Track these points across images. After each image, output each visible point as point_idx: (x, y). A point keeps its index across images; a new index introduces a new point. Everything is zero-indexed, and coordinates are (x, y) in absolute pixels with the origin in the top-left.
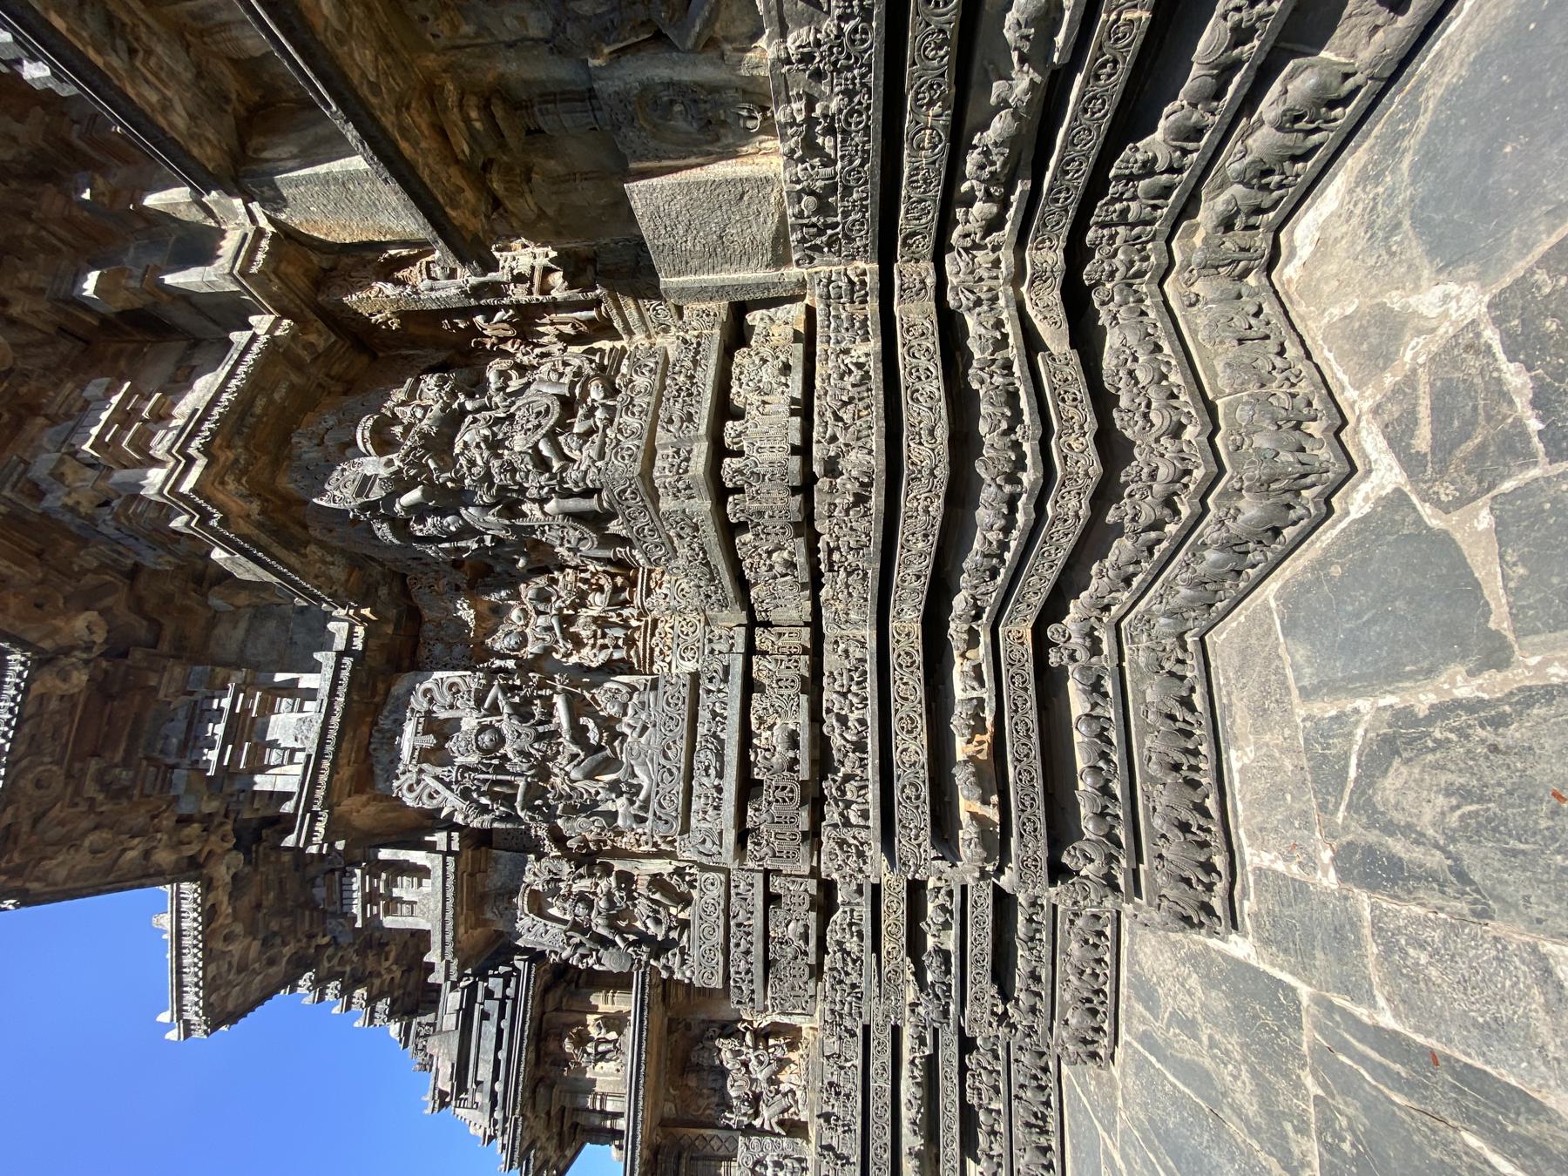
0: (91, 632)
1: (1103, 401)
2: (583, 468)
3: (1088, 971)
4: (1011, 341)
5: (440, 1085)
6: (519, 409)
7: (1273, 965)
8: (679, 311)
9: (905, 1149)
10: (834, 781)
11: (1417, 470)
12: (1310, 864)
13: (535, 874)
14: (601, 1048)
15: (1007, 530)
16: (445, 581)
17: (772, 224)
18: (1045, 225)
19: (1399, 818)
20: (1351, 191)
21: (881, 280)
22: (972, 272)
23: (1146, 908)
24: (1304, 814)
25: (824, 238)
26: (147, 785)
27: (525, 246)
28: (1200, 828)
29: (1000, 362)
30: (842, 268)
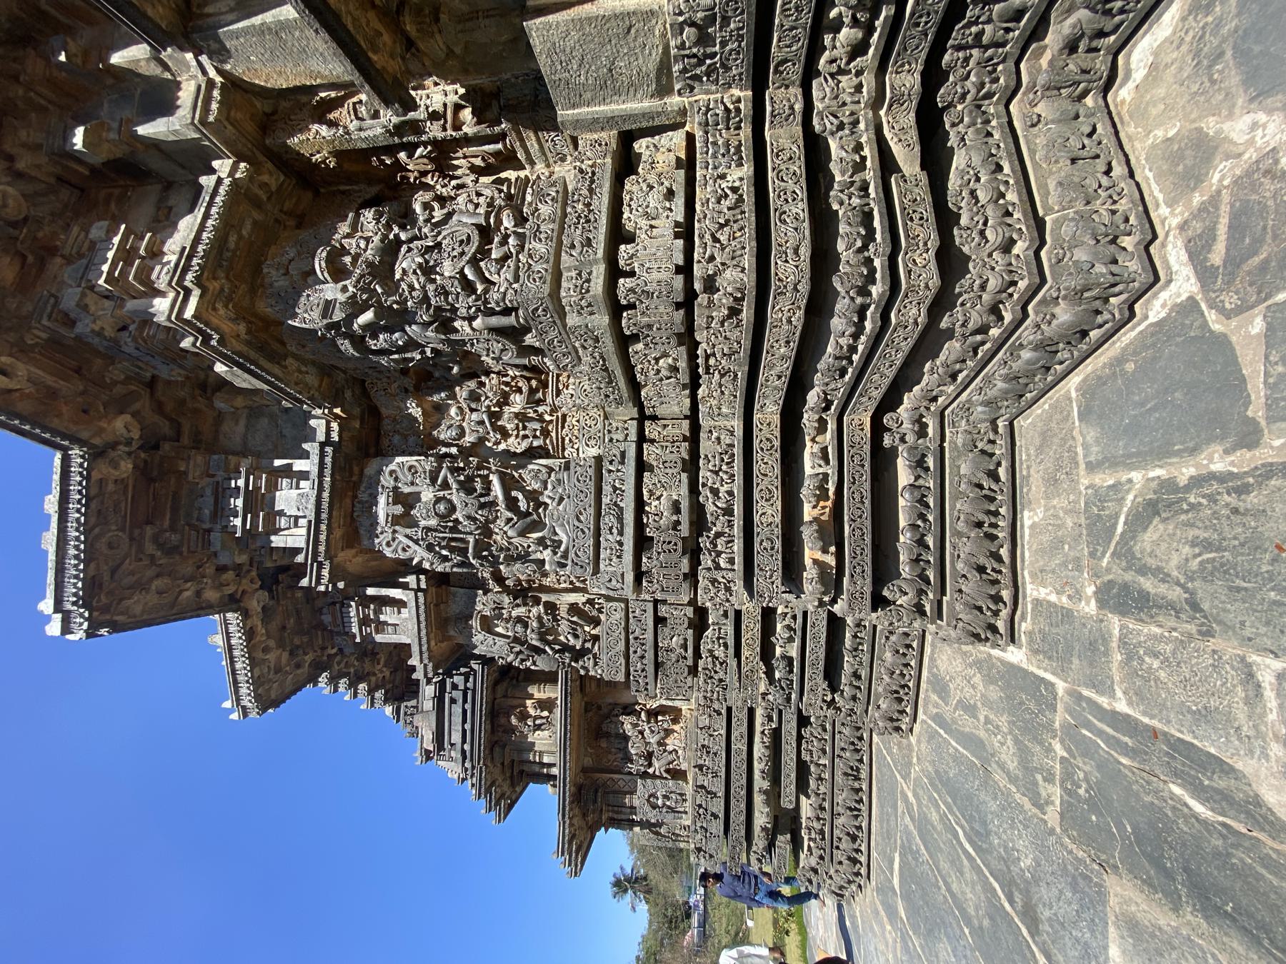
0: (129, 431)
2: (502, 290)
3: (898, 672)
4: (869, 163)
5: (425, 745)
6: (444, 238)
7: (1039, 667)
8: (575, 141)
9: (756, 789)
10: (708, 537)
11: (1209, 281)
12: (1077, 596)
13: (483, 604)
14: (538, 722)
15: (855, 336)
16: (396, 385)
17: (656, 55)
18: (905, 49)
19: (1152, 562)
21: (754, 107)
22: (836, 97)
23: (946, 627)
24: (1077, 560)
25: (704, 68)
26: (192, 544)
27: (436, 84)
28: (993, 570)
29: (857, 185)
30: (719, 95)
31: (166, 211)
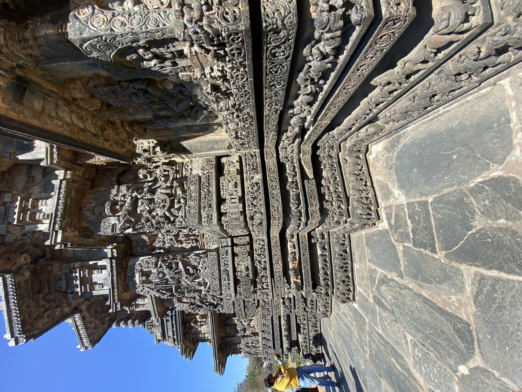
1: (321, 197)
5: (158, 338)
9: (283, 335)
20: (384, 149)
29: (295, 184)
31: (31, 178)
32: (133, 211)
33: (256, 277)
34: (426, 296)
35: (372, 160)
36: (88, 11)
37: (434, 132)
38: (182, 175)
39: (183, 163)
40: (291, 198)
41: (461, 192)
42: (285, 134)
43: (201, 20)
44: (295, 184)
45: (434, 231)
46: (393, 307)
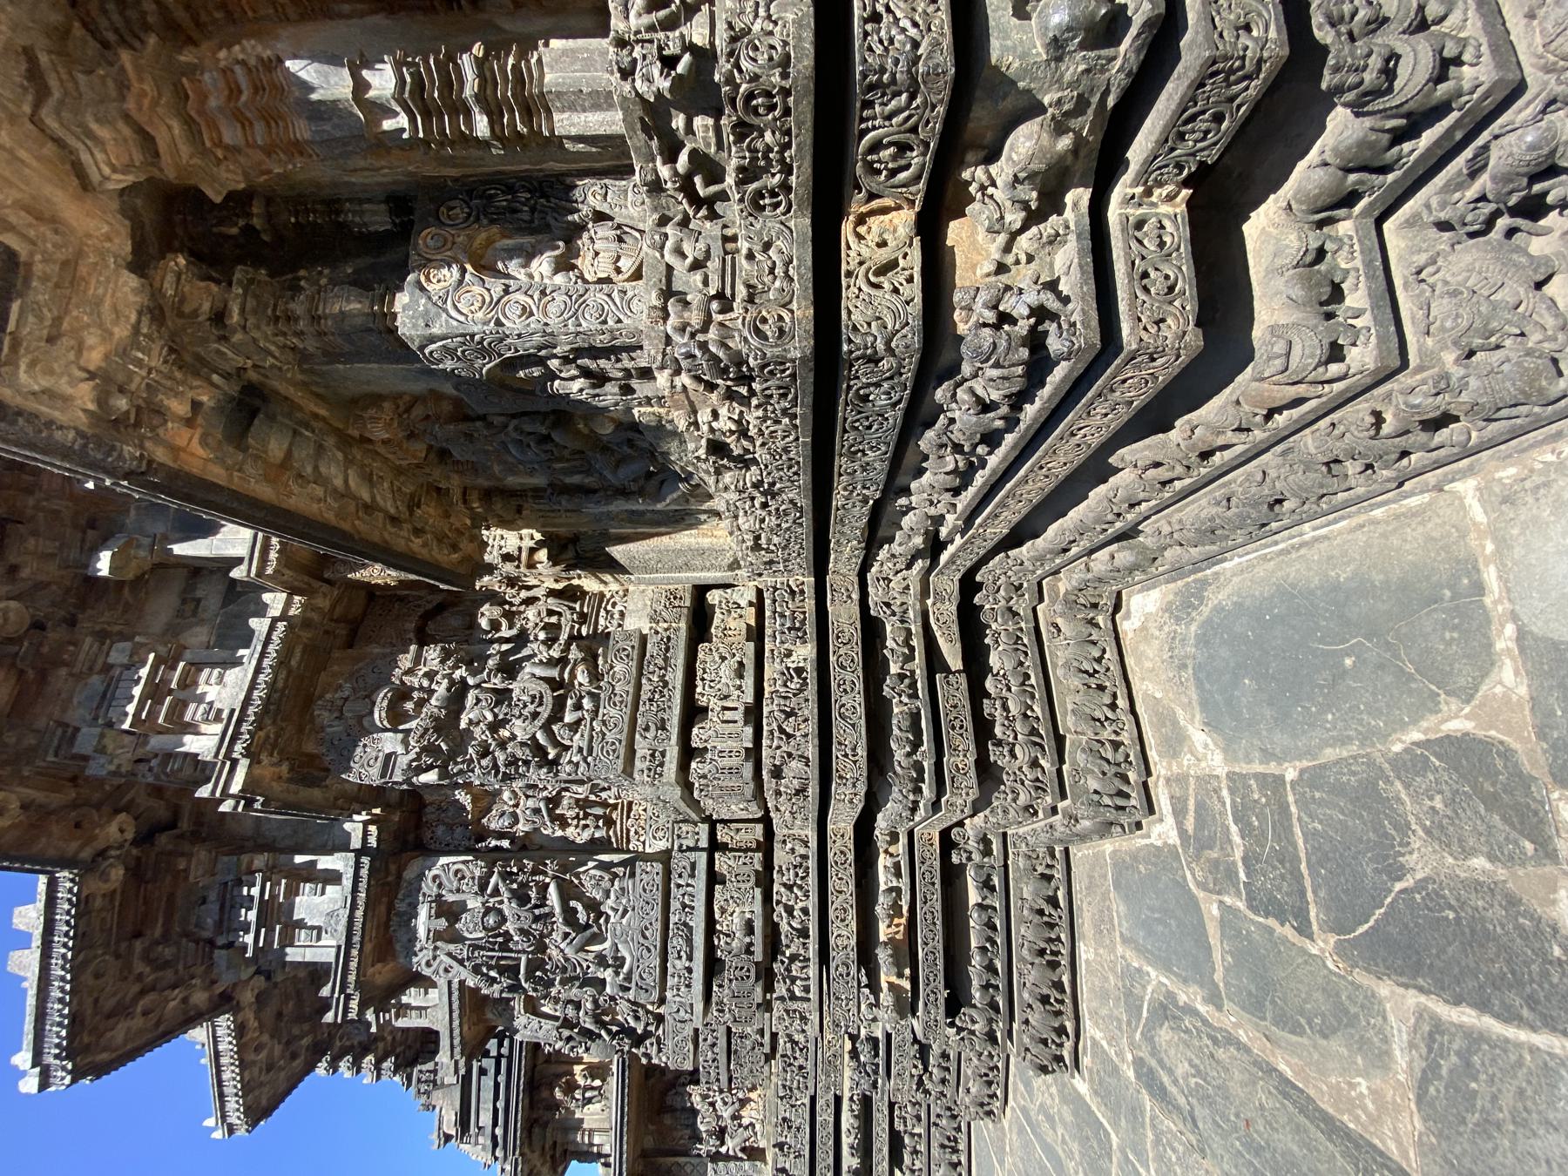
1: (983, 730)
9: (845, 1168)
14: (588, 1095)
32: (447, 724)
33: (774, 959)
34: (1289, 1073)
35: (1130, 635)
36: (450, 275)
37: (1293, 586)
38: (596, 628)
39: (602, 595)
40: (894, 721)
41: (1371, 763)
42: (886, 547)
43: (705, 329)
44: (907, 681)
45: (1303, 866)
46: (1194, 1101)
